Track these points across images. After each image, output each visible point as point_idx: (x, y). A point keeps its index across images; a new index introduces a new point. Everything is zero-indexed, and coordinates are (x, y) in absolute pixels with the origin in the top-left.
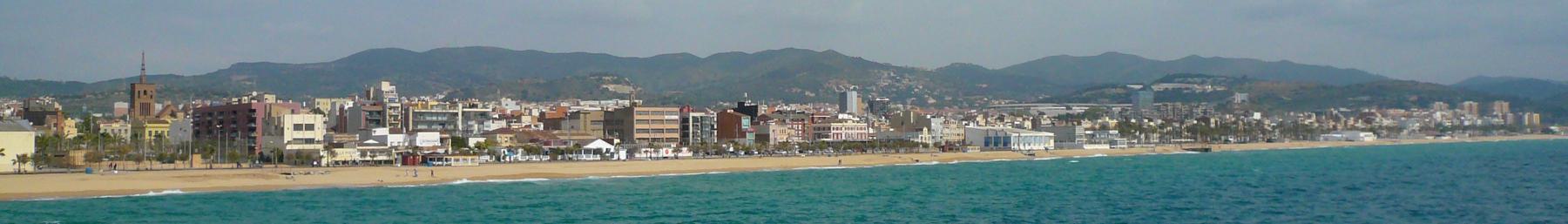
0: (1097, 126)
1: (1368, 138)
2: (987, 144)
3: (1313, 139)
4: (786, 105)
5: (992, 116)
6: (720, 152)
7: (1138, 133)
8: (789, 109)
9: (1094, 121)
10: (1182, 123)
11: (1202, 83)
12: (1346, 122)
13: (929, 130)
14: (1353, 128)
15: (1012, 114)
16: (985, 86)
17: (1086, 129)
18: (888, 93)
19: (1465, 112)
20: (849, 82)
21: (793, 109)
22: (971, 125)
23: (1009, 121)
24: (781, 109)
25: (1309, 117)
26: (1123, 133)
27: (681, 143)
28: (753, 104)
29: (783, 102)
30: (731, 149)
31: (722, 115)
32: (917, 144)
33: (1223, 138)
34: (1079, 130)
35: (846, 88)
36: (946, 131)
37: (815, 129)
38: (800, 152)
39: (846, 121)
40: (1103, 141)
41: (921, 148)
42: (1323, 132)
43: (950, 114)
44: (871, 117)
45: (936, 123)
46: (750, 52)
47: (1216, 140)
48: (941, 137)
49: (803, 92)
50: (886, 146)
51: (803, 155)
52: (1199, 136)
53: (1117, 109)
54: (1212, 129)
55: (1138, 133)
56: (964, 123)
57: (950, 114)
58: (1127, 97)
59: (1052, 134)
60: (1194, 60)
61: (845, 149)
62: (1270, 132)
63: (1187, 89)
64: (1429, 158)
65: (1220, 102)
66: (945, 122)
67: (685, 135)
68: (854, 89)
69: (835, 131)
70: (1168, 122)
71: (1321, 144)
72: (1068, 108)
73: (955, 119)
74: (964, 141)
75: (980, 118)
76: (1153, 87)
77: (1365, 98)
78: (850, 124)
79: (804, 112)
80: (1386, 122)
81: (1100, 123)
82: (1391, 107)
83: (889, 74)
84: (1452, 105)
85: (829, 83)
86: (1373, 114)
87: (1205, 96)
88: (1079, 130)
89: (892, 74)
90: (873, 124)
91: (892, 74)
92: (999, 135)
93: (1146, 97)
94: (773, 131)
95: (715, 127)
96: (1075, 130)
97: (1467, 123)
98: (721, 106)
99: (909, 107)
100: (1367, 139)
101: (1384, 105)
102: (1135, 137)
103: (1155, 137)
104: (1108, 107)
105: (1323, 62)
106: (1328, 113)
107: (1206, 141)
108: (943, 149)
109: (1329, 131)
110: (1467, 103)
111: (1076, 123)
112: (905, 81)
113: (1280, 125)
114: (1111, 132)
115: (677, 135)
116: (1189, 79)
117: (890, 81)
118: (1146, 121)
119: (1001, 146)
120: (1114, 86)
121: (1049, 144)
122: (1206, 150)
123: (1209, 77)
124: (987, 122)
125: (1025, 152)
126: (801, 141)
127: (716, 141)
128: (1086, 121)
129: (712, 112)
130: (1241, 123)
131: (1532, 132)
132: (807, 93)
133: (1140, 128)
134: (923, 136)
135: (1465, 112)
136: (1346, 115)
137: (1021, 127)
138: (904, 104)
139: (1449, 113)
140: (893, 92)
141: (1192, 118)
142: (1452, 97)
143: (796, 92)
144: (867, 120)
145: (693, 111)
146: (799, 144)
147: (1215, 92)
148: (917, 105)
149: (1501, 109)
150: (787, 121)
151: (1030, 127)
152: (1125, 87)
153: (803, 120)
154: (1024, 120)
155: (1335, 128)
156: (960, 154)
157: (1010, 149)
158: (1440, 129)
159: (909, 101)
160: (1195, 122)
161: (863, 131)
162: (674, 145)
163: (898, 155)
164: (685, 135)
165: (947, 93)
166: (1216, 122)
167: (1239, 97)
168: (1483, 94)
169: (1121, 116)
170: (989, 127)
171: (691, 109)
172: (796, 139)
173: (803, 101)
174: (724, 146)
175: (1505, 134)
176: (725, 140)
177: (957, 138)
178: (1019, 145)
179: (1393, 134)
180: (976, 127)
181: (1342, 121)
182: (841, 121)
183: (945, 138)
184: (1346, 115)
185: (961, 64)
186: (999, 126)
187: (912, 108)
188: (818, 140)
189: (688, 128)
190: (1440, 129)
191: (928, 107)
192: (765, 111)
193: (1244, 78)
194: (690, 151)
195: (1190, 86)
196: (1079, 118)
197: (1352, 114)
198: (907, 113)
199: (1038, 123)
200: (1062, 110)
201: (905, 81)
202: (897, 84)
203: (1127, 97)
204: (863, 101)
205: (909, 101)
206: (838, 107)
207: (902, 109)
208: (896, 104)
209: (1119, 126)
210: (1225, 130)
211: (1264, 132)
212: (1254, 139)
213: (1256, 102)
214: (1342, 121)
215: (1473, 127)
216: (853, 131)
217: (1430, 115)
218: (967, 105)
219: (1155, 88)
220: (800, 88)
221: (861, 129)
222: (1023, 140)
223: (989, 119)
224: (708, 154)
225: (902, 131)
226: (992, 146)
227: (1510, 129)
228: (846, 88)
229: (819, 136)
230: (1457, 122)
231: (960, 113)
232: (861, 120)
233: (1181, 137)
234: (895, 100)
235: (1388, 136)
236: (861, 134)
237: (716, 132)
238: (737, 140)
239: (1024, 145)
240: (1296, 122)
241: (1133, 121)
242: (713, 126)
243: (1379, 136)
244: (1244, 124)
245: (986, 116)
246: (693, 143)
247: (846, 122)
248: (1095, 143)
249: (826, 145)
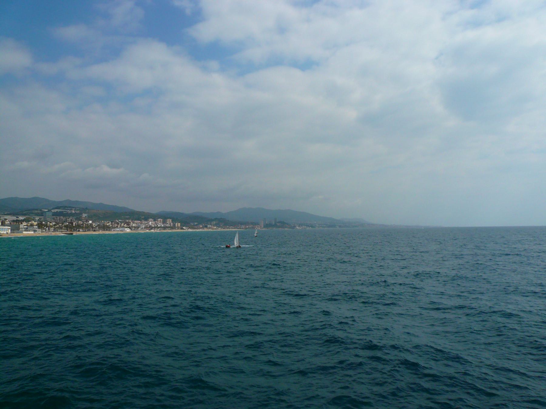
0: (29, 225)
1: (128, 230)
3: (109, 230)
7: (45, 227)
10: (63, 224)
11: (71, 210)
12: (121, 225)
14: (123, 227)
19: (159, 222)
25: (109, 223)
26: (39, 227)
33: (78, 230)
34: (21, 226)
42: (113, 228)
47: (75, 230)
52: (69, 229)
53: (37, 218)
54: (74, 227)
55: (45, 227)
58: (42, 214)
59: (10, 227)
60: (69, 201)
62: (95, 228)
63: (66, 212)
64: (147, 237)
65: (77, 217)
70: (57, 224)
71: (112, 232)
72: (17, 217)
76: (52, 210)
77: (127, 217)
80: (134, 225)
81: (30, 224)
82: (136, 220)
84: (155, 220)
86: (130, 222)
87: (71, 215)
93: (51, 214)
97: (159, 226)
100: (127, 231)
101: (134, 219)
102: (44, 229)
103: (52, 229)
104: (34, 218)
105: (114, 204)
106: (115, 221)
107: (71, 231)
109: (115, 228)
110: (159, 219)
113: (98, 225)
114: (34, 227)
116: (66, 208)
118: (49, 223)
120: (37, 210)
122: (71, 234)
123: (74, 208)
128: (25, 222)
130: (84, 224)
131: (178, 229)
133: (46, 226)
135: (159, 222)
136: (121, 222)
139: (154, 223)
141: (66, 222)
142: (155, 217)
147: (75, 213)
149: (169, 221)
152: (41, 210)
155: (117, 227)
158: (151, 228)
160: (68, 224)
166: (75, 224)
167: (84, 215)
168: (164, 217)
169: (39, 221)
175: (170, 229)
179: (136, 229)
181: (120, 224)
184: (121, 222)
190: (151, 228)
193: (86, 208)
195: (66, 211)
196: (22, 221)
197: (123, 222)
199: (4, 223)
200: (14, 218)
203: (42, 214)
209: (38, 225)
210: (78, 227)
211: (93, 228)
212: (89, 230)
213: (90, 218)
214: (120, 224)
215: (161, 227)
217: (148, 223)
219: (53, 211)
227: (172, 228)
230: (156, 226)
233: (62, 229)
235: (134, 230)
240: (104, 224)
241: (44, 223)
243: (131, 230)
244: (86, 225)
248: (28, 231)
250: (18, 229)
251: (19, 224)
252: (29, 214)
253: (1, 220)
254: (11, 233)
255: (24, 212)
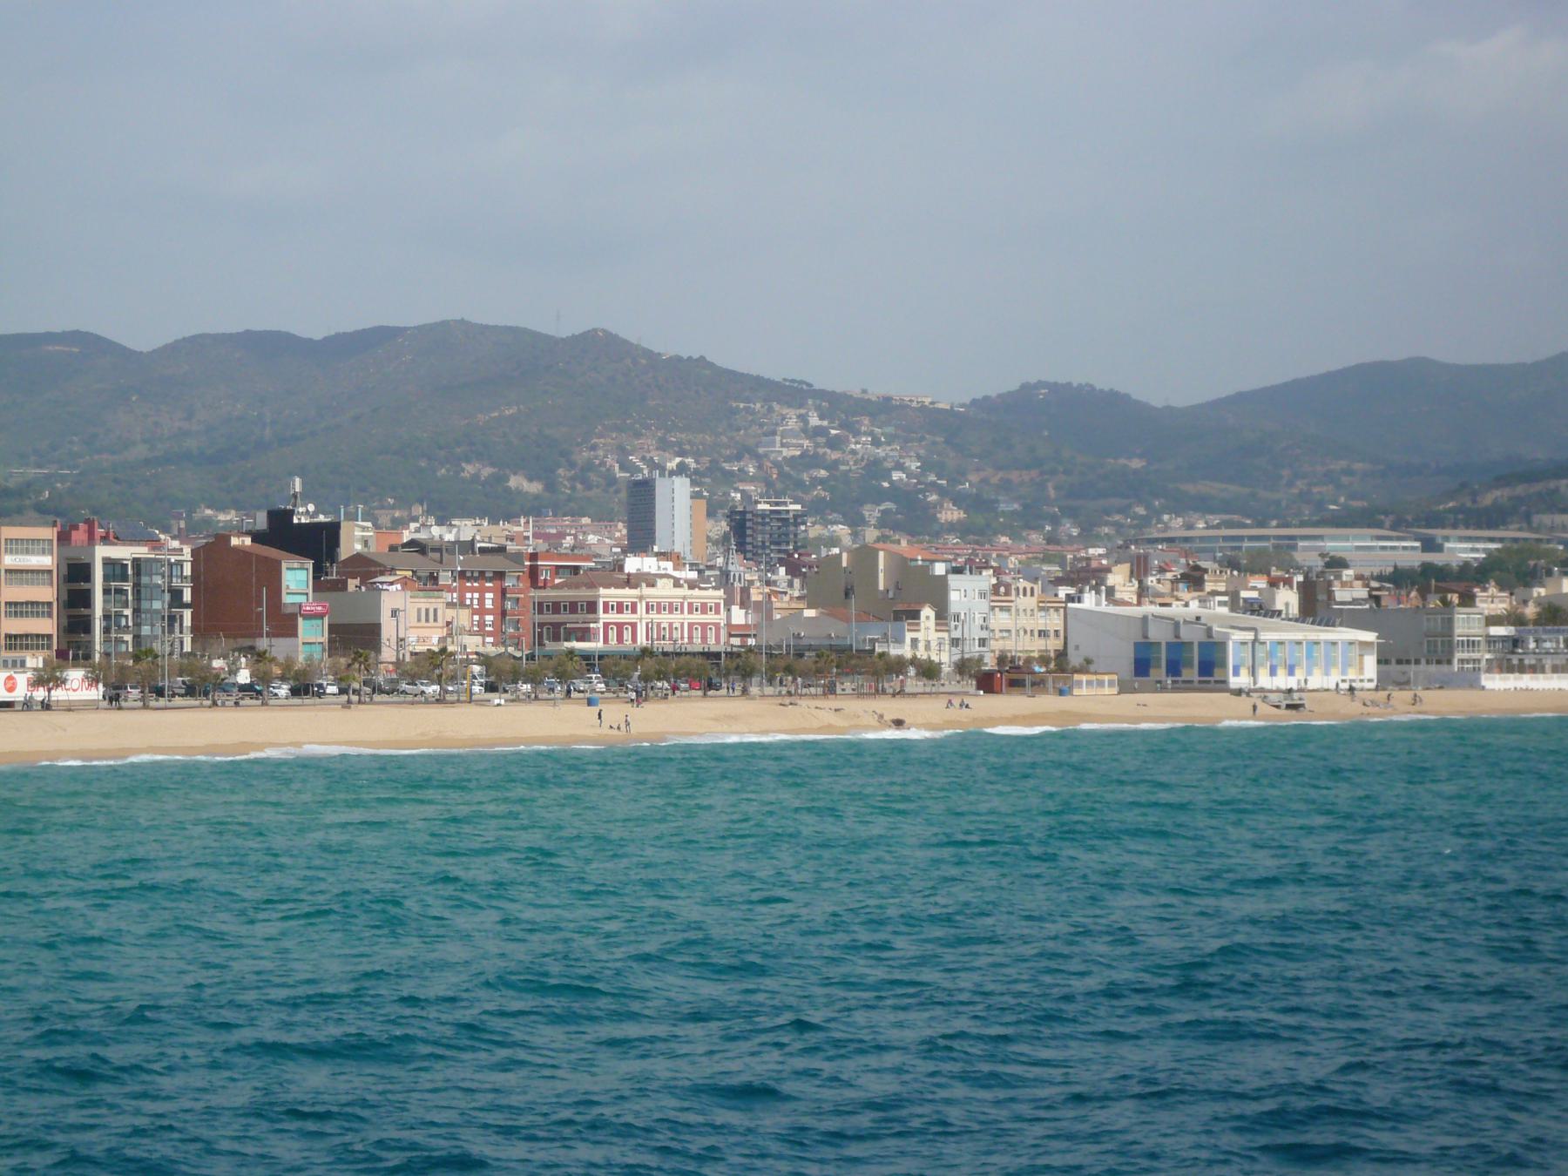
0: (1530, 611)
2: (1142, 666)
4: (440, 523)
5: (1162, 570)
6: (203, 687)
8: (449, 537)
9: (1520, 591)
13: (942, 616)
15: (1233, 564)
16: (1136, 464)
17: (1492, 620)
18: (799, 484)
20: (663, 445)
21: (466, 536)
22: (1089, 601)
23: (1222, 587)
24: (422, 536)
27: (61, 654)
28: (321, 518)
29: (428, 513)
30: (244, 677)
31: (212, 555)
32: (898, 666)
34: (1466, 624)
35: (653, 465)
36: (1001, 620)
37: (540, 607)
38: (491, 688)
39: (650, 580)
40: (1548, 662)
41: (913, 683)
43: (1013, 561)
44: (737, 566)
45: (966, 593)
46: (314, 327)
48: (983, 642)
49: (500, 479)
50: (789, 670)
51: (497, 699)
56: (1063, 591)
57: (1013, 561)
59: (1370, 636)
61: (645, 678)
66: (995, 589)
67: (76, 623)
68: (681, 470)
69: (613, 617)
72: (1430, 545)
73: (1035, 580)
74: (1062, 655)
75: (1118, 577)
78: (664, 590)
79: (501, 550)
81: (1538, 602)
83: (803, 419)
85: (594, 448)
88: (1466, 624)
89: (814, 421)
90: (745, 592)
91: (814, 421)
92: (1186, 634)
94: (394, 613)
95: (187, 596)
96: (1449, 623)
98: (207, 521)
99: (871, 534)
108: (987, 683)
111: (1455, 598)
112: (860, 445)
115: (47, 626)
117: (806, 443)
119: (1191, 674)
121: (1361, 669)
124: (1142, 592)
125: (1273, 697)
126: (491, 650)
127: (187, 648)
128: (1493, 590)
129: (175, 544)
132: (515, 482)
134: (920, 636)
137: (1259, 608)
138: (856, 522)
140: (816, 482)
143: (476, 477)
144: (725, 579)
145: (105, 540)
146: (485, 660)
148: (896, 527)
150: (445, 578)
151: (1294, 610)
153: (500, 576)
154: (1273, 583)
156: (1046, 702)
157: (1222, 686)
159: (872, 513)
161: (710, 617)
162: (35, 660)
163: (832, 703)
164: (76, 623)
165: (1006, 486)
170: (1149, 609)
171: (100, 531)
172: (473, 643)
173: (501, 508)
174: (217, 663)
176: (224, 643)
177: (1035, 646)
178: (1253, 673)
180: (1105, 607)
182: (631, 581)
183: (997, 645)
185: (1054, 388)
186: (1186, 606)
187: (883, 539)
188: (550, 646)
189: (85, 599)
191: (937, 535)
192: (366, 543)
194: (94, 681)
196: (1467, 580)
198: (865, 556)
199: (1322, 597)
200: (1406, 552)
201: (860, 445)
202: (835, 455)
204: (711, 514)
205: (872, 513)
206: (621, 530)
207: (847, 540)
208: (826, 523)
216: (676, 618)
218: (1075, 532)
220: (492, 465)
221: (704, 609)
222: (1271, 655)
223: (1151, 581)
224: (160, 692)
225: (848, 620)
226: (1159, 673)
228: (653, 465)
229: (557, 632)
231: (1047, 559)
232: (703, 578)
234: (818, 509)
236: (704, 626)
237: (187, 614)
238: (263, 643)
239: (1273, 672)
242: (176, 594)
245: (1140, 569)
246: (107, 655)
247: (653, 585)
248: (1522, 669)
249: (578, 664)
250: (1439, 648)
251: (1446, 603)
252: (1527, 518)
253: (1298, 568)
254: (1383, 682)
255: (1488, 499)
